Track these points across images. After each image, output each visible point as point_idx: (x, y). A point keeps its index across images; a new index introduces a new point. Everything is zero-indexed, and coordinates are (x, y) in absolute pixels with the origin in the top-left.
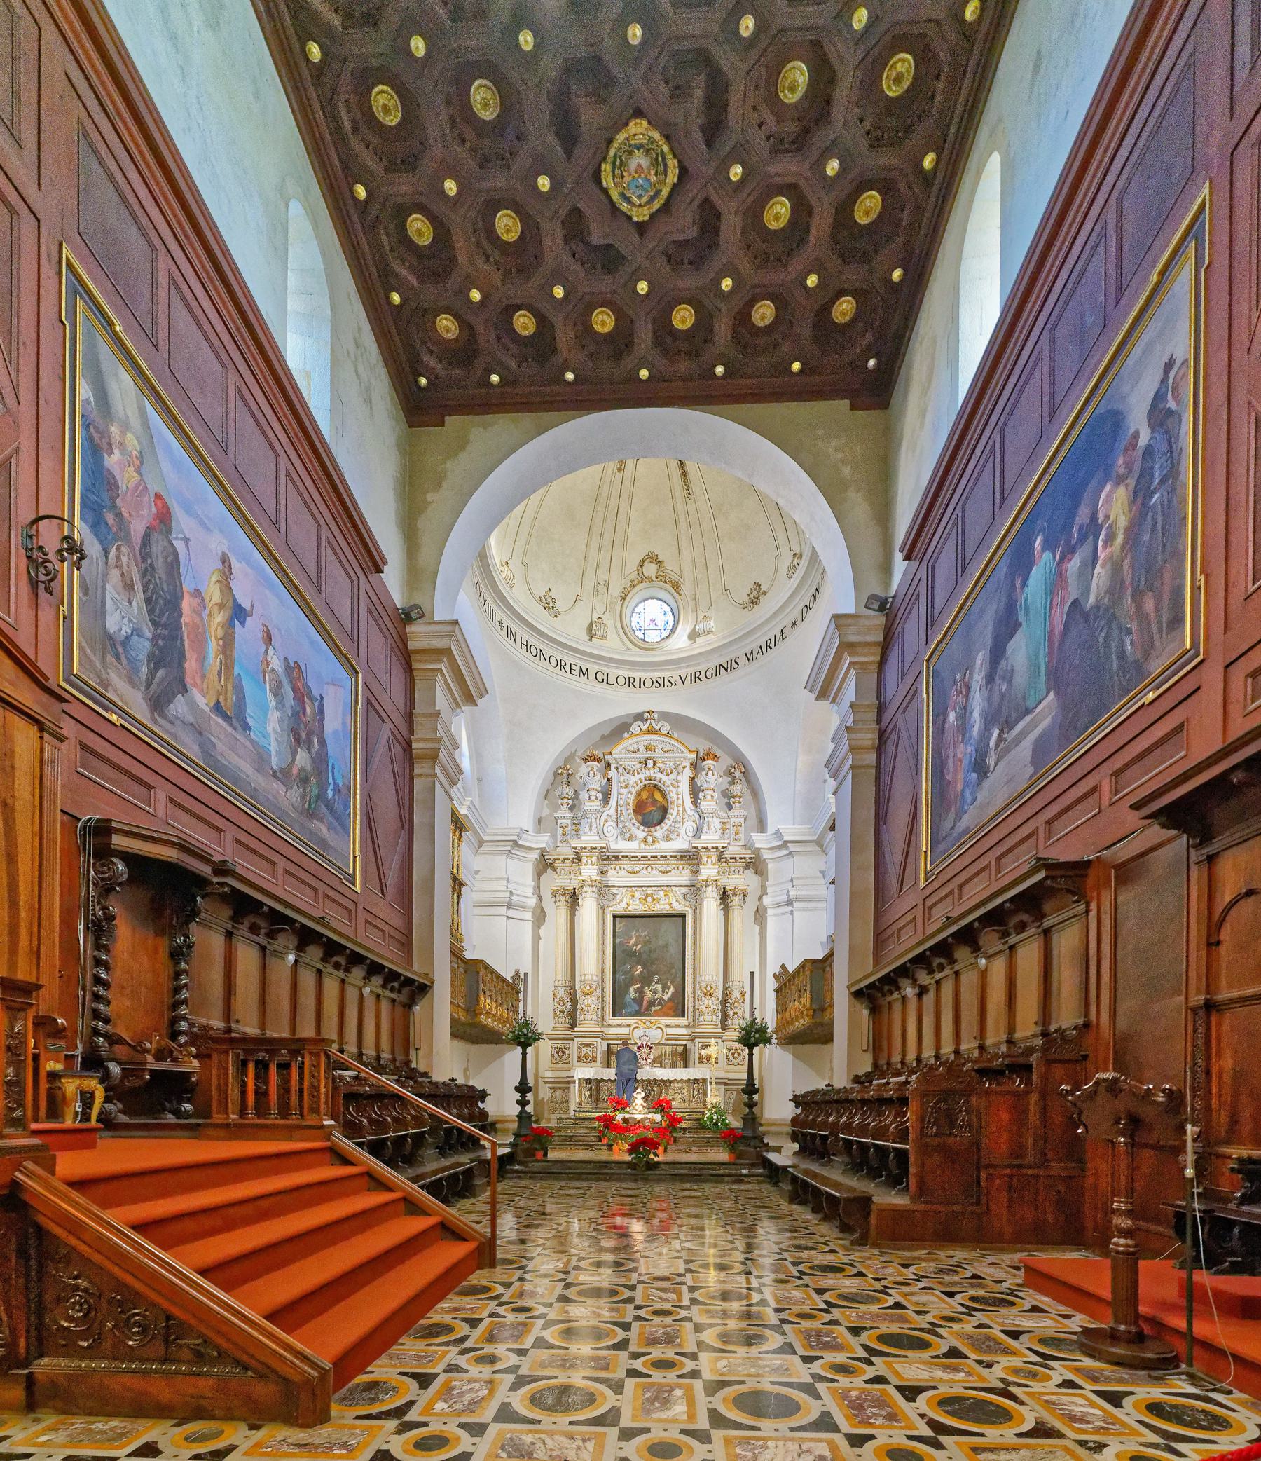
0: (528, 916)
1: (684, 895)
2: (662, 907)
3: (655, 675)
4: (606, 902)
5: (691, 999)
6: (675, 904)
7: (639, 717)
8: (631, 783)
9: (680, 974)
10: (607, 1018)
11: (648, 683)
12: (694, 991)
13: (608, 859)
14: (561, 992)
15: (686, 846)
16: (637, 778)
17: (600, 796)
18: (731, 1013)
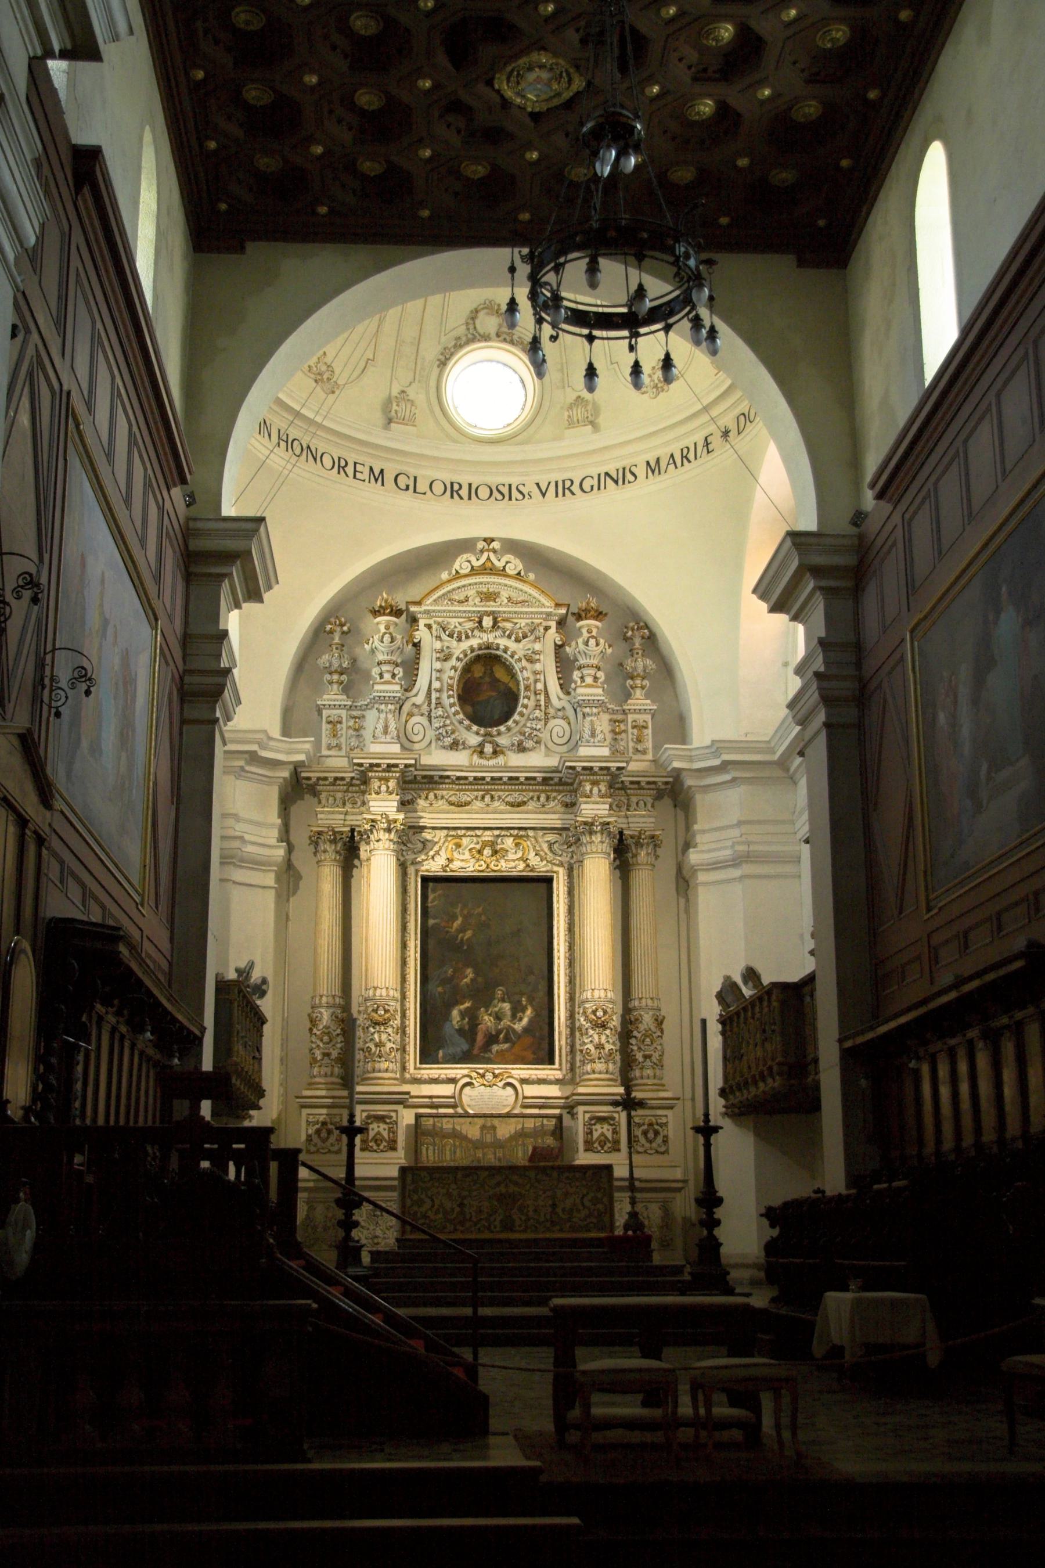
0: (270, 879)
1: (551, 845)
2: (510, 864)
3: (494, 480)
4: (410, 857)
5: (565, 1031)
6: (534, 860)
7: (465, 545)
8: (457, 653)
9: (543, 986)
10: (411, 1066)
11: (484, 492)
12: (572, 1016)
13: (414, 780)
14: (325, 1016)
15: (553, 762)
16: (465, 645)
17: (399, 671)
18: (639, 1057)
